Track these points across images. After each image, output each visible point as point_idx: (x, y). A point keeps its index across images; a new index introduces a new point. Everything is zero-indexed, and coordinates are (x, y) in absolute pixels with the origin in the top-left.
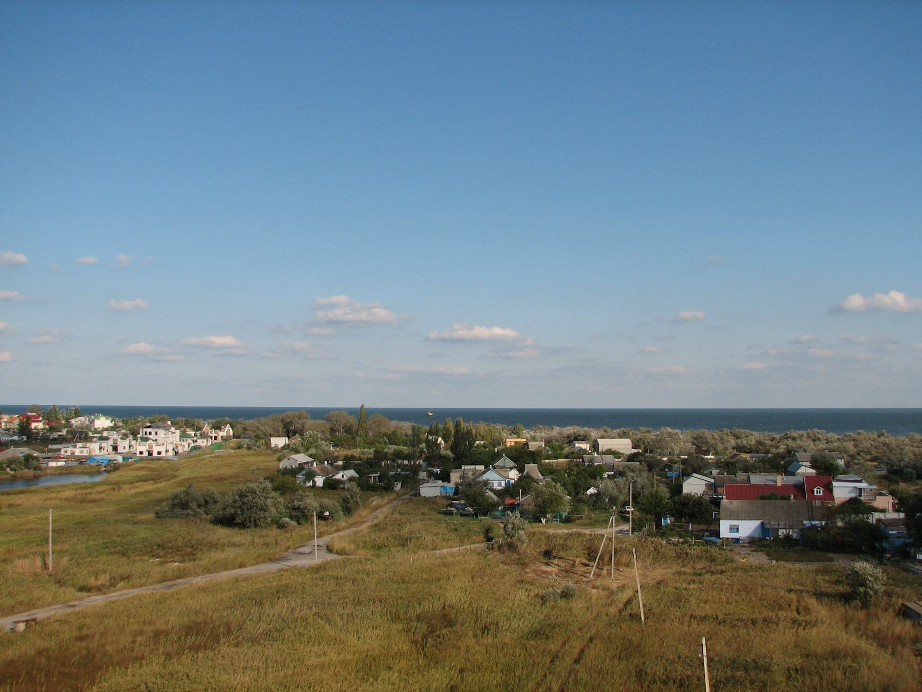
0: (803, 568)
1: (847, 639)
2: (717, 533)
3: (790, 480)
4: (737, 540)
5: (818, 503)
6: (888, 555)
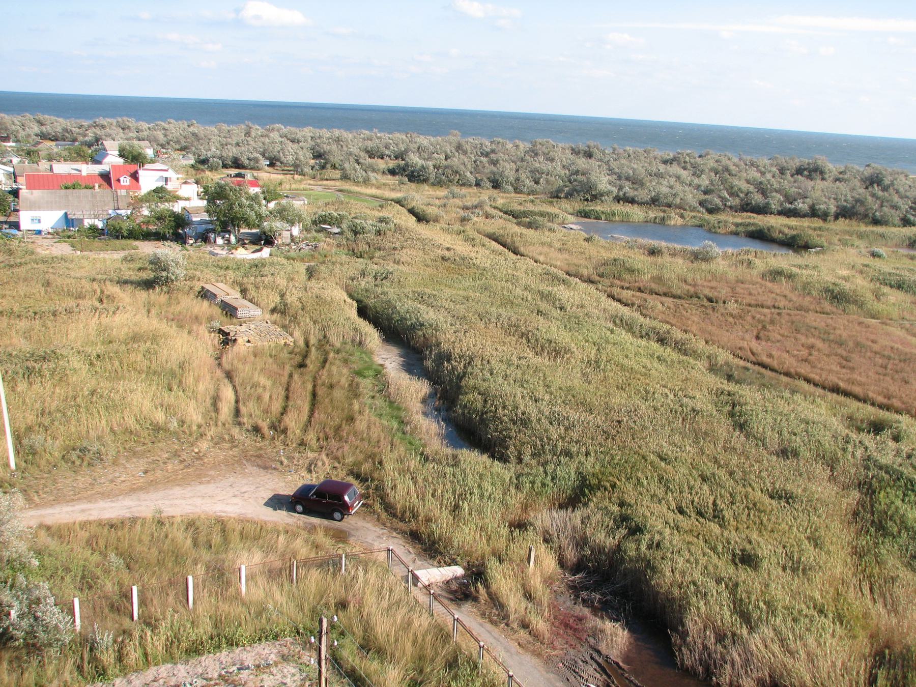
0: (107, 256)
1: (152, 324)
2: (16, 226)
3: (96, 169)
4: (39, 232)
5: (123, 192)
6: (191, 242)
